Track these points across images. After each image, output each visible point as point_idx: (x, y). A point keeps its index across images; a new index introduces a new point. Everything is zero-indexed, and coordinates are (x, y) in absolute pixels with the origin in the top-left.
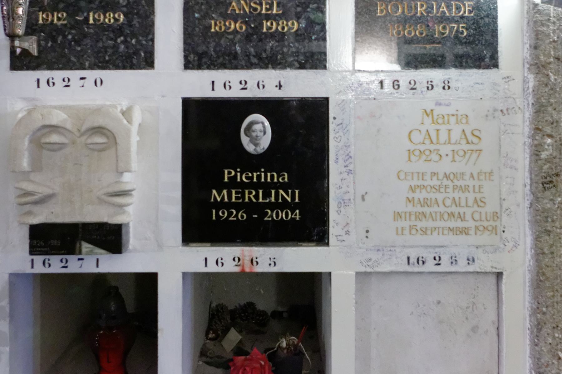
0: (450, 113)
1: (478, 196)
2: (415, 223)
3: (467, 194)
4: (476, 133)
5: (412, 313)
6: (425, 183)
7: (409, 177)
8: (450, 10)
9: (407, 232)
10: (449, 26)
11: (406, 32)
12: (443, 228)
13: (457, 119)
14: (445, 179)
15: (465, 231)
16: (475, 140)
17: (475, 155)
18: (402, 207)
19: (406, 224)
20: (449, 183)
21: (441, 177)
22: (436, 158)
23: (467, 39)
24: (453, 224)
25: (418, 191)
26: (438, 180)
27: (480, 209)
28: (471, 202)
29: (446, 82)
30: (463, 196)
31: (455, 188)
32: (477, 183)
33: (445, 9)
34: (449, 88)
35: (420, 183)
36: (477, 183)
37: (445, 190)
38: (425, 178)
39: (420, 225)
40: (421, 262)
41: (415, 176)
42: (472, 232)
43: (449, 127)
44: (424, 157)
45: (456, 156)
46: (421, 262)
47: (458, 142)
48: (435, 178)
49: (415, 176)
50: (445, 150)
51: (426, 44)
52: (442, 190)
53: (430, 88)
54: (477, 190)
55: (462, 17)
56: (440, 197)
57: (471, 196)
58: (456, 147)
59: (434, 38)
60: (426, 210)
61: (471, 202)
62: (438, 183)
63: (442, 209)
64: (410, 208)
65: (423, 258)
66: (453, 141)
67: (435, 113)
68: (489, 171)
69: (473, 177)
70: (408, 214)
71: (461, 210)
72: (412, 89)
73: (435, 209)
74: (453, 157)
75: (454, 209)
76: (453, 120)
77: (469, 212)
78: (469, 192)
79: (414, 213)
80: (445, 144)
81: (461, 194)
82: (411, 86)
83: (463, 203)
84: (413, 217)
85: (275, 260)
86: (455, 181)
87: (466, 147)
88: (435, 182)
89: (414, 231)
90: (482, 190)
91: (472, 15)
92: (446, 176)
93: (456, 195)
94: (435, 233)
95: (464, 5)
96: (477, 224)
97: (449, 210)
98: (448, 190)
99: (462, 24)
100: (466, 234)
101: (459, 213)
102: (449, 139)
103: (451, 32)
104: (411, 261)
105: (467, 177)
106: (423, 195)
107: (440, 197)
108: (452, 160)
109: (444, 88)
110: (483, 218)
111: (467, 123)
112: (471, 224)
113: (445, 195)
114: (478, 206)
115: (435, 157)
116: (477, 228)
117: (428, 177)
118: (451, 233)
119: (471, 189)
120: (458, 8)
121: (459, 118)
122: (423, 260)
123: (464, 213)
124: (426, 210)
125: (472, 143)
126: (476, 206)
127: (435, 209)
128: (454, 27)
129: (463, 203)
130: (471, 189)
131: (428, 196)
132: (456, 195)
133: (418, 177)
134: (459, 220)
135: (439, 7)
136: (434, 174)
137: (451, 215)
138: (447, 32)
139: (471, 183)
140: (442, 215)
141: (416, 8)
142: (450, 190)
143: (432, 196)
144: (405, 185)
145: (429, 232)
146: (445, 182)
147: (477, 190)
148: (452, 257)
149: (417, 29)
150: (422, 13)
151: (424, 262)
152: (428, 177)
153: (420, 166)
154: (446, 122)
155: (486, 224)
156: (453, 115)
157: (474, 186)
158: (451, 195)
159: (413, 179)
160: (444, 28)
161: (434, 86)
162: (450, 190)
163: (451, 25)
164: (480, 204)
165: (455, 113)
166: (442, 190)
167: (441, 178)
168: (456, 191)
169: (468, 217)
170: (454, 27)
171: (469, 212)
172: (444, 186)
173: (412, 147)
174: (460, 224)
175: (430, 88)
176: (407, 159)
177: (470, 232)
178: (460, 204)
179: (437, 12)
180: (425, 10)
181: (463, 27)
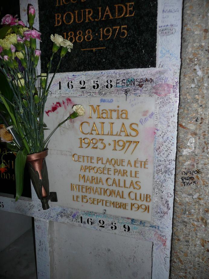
0: (112, 108)
1: (135, 180)
2: (85, 194)
3: (125, 178)
4: (134, 126)
5: (91, 252)
6: (93, 165)
7: (81, 160)
8: (113, 14)
9: (80, 199)
10: (112, 29)
11: (77, 38)
12: (106, 201)
13: (118, 114)
14: (108, 164)
15: (123, 206)
16: (133, 133)
17: (132, 146)
18: (76, 182)
19: (80, 194)
20: (111, 167)
21: (104, 161)
22: (101, 146)
23: (127, 40)
24: (113, 199)
25: (87, 170)
26: (102, 164)
27: (135, 191)
28: (128, 184)
29: (109, 82)
30: (122, 179)
31: (115, 171)
32: (134, 170)
33: (109, 13)
34: (111, 86)
35: (89, 164)
36: (134, 170)
37: (108, 173)
38: (93, 161)
39: (89, 196)
40: (90, 223)
41: (85, 158)
42: (129, 207)
43: (112, 121)
44: (92, 145)
45: (117, 146)
46: (90, 223)
47: (118, 134)
48: (100, 162)
49: (85, 158)
50: (108, 140)
51: (93, 48)
52: (106, 172)
53: (96, 87)
54: (133, 175)
55: (124, 18)
56: (104, 177)
57: (129, 180)
58: (117, 138)
59: (99, 41)
60: (94, 185)
61: (128, 184)
62: (103, 166)
63: (105, 186)
64: (82, 183)
65: (91, 220)
66: (114, 133)
67: (101, 108)
68: (144, 160)
69: (130, 164)
70: (80, 187)
71: (121, 190)
72: (83, 88)
73: (100, 185)
74: (115, 147)
75: (114, 188)
76: (114, 115)
77: (126, 192)
78: (127, 176)
79: (85, 187)
80: (108, 135)
81: (120, 177)
82: (82, 86)
83: (122, 184)
84: (84, 190)
85: (3, 204)
86: (116, 166)
87: (125, 139)
88: (100, 165)
89: (85, 200)
90: (137, 175)
91: (133, 15)
92: (109, 161)
93: (117, 177)
94: (100, 204)
95: (126, 6)
96: (133, 202)
97: (111, 188)
98: (110, 172)
99: (123, 25)
100: (123, 208)
101: (118, 192)
102: (112, 132)
103: (113, 34)
104: (83, 220)
105: (125, 164)
106: (92, 174)
107: (104, 177)
108: (113, 148)
109: (107, 87)
110: (138, 198)
111: (127, 118)
112: (127, 201)
113: (107, 176)
114: (134, 188)
115: (100, 145)
116: (132, 205)
117: (95, 161)
118: (112, 206)
119: (129, 174)
120: (121, 10)
121: (120, 113)
122: (92, 221)
123: (123, 192)
124: (94, 185)
125: (130, 135)
126: (132, 187)
127: (100, 185)
128: (116, 29)
129: (122, 184)
130: (129, 174)
131: (96, 175)
132: (117, 177)
133: (88, 160)
134: (118, 197)
135: (103, 11)
136: (99, 159)
137: (112, 193)
138: (111, 34)
139: (128, 169)
140: (105, 191)
141: (85, 16)
142: (112, 172)
143: (99, 175)
144: (78, 165)
145: (96, 202)
146: (108, 166)
147: (133, 175)
148: (112, 223)
149: (86, 35)
150: (89, 19)
151: (92, 223)
152: (95, 161)
153: (89, 152)
154: (109, 117)
155: (140, 203)
156: (115, 111)
157: (131, 171)
158: (112, 177)
159: (84, 161)
160: (108, 31)
161: (100, 85)
162: (112, 172)
163: (114, 28)
164: (136, 186)
165: (116, 108)
166: (106, 172)
167: (104, 161)
168: (117, 174)
169: (126, 195)
170: (116, 29)
171: (126, 192)
172: (107, 169)
173: (83, 136)
174: (118, 200)
175: (96, 87)
176: (79, 145)
177: (127, 207)
178: (119, 184)
179: (102, 17)
180: (91, 16)
181: (124, 29)
